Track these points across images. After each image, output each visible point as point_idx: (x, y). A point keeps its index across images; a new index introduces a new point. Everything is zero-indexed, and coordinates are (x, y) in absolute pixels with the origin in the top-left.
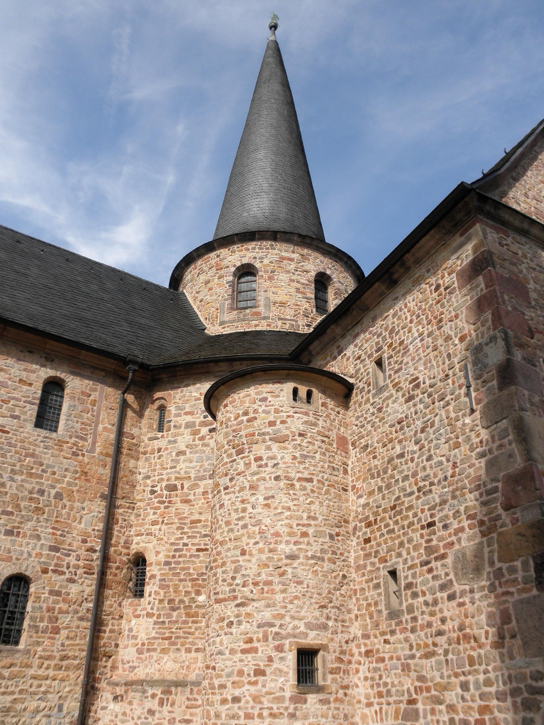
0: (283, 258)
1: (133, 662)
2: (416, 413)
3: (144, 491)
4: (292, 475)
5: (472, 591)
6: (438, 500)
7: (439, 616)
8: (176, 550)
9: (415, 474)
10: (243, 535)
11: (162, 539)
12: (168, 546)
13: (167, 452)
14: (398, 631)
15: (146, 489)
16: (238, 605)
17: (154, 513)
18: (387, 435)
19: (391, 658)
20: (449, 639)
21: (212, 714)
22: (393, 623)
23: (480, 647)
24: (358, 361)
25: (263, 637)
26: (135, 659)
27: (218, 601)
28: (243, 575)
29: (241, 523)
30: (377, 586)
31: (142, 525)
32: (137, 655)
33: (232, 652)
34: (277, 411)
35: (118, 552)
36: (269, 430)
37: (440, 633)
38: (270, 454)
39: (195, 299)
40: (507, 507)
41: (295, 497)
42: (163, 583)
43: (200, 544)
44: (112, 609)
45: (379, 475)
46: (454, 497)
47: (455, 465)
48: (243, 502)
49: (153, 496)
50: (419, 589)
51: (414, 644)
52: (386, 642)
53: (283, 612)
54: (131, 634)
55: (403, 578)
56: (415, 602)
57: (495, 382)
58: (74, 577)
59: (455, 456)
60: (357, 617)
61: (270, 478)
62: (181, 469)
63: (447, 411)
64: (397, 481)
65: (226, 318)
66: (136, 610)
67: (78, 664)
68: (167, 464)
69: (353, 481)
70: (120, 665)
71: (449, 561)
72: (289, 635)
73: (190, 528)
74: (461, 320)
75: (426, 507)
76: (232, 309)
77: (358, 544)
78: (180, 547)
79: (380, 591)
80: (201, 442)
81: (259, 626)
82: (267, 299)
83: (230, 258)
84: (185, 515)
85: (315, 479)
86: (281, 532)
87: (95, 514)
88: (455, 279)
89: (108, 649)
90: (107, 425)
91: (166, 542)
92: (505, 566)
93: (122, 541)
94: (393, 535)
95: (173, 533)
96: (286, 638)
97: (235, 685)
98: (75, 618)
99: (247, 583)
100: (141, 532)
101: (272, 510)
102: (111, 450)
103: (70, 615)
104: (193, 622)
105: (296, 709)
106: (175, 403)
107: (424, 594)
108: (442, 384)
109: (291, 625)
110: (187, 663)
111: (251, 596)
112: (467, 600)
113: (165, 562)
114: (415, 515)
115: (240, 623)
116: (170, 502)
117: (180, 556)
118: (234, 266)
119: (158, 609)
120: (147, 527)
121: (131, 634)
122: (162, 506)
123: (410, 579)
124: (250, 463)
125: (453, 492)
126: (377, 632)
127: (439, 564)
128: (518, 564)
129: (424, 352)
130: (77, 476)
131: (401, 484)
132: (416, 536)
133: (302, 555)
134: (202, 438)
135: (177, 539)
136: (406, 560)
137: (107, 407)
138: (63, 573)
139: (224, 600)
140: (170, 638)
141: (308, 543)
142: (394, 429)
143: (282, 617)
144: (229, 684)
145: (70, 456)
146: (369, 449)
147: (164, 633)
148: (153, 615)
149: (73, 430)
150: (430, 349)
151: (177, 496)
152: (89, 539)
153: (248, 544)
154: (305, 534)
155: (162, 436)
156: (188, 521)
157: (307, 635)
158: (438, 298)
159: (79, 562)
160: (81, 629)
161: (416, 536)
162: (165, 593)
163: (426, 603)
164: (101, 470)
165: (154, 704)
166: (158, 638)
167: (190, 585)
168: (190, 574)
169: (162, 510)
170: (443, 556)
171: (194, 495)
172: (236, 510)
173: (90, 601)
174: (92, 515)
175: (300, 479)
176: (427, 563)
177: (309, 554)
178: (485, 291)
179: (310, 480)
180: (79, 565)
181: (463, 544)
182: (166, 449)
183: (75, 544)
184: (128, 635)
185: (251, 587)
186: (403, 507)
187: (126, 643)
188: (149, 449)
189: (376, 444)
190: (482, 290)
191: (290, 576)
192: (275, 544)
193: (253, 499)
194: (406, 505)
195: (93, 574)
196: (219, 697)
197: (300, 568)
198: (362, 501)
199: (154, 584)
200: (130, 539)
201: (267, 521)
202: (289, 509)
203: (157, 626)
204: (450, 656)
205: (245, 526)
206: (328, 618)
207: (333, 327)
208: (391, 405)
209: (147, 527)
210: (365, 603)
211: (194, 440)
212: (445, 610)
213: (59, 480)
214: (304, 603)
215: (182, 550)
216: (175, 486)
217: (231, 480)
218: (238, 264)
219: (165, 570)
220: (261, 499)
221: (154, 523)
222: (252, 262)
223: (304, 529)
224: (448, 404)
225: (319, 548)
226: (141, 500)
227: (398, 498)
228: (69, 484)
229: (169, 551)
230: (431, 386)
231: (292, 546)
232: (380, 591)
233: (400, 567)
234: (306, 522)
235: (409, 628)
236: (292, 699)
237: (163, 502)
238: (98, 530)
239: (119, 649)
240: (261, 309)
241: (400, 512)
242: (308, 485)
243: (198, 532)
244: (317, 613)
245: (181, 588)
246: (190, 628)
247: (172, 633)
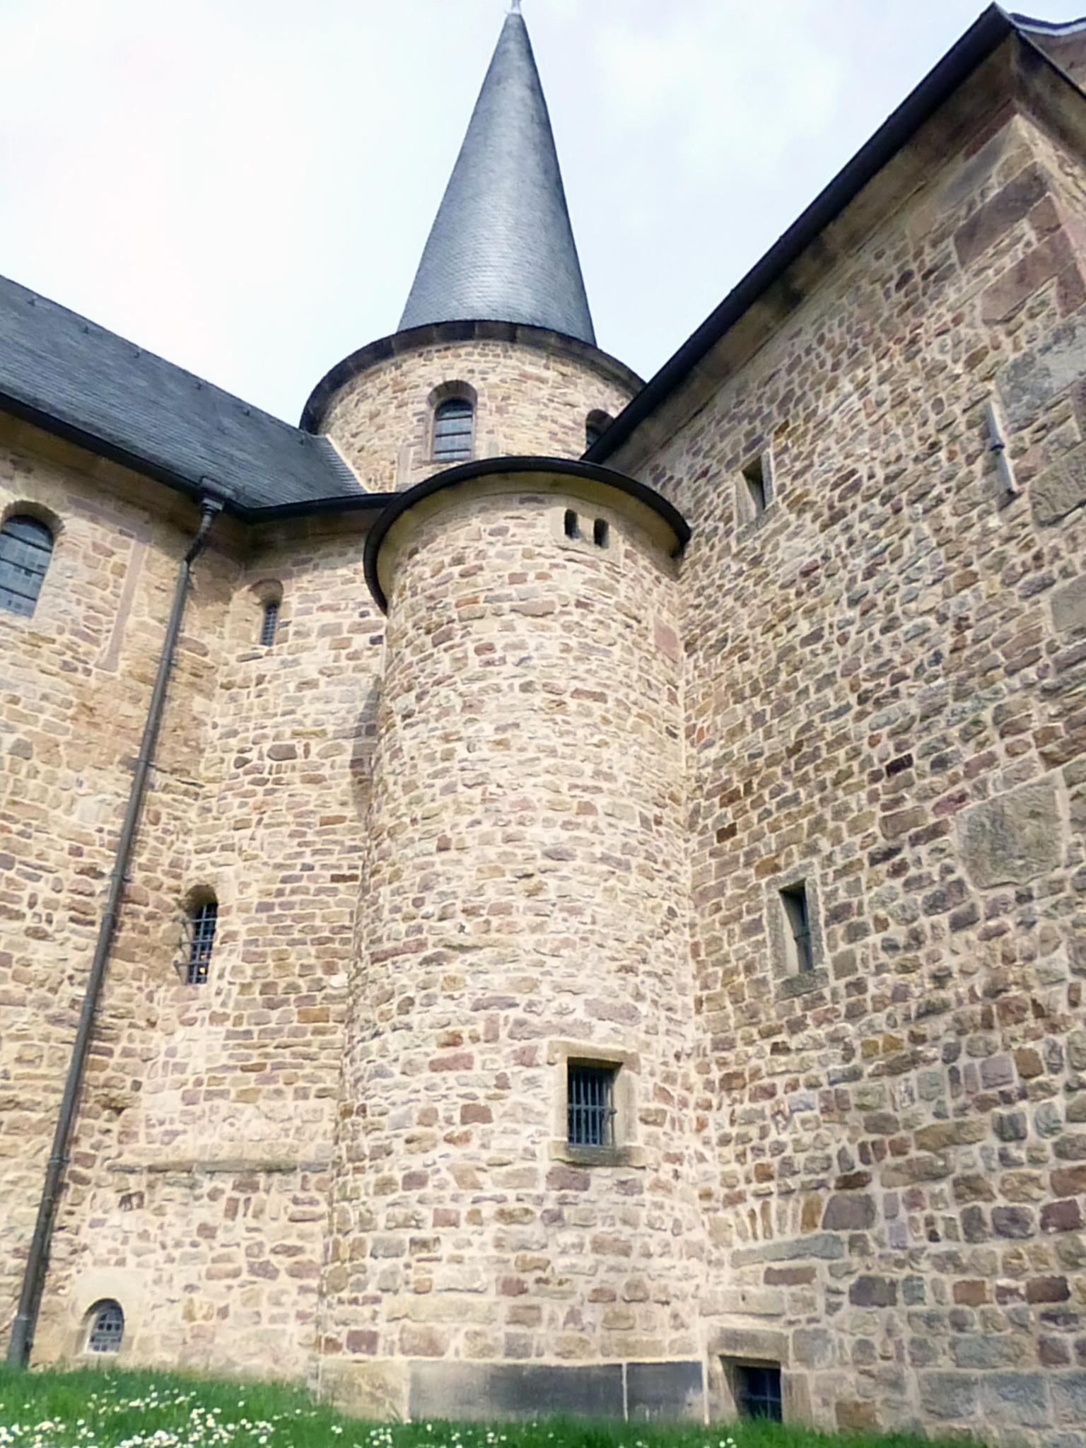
0: (525, 377)
1: (172, 1121)
2: (851, 542)
3: (222, 761)
4: (561, 683)
5: (1024, 898)
6: (915, 710)
7: (926, 969)
8: (284, 881)
10: (445, 807)
11: (255, 857)
12: (268, 871)
13: (276, 683)
14: (809, 1021)
15: (226, 756)
16: (427, 961)
17: (243, 805)
18: (774, 605)
19: (793, 1086)
20: (957, 1020)
21: (354, 1217)
22: (798, 1002)
23: (1054, 1028)
24: (703, 481)
25: (486, 1032)
26: (176, 1116)
27: (376, 959)
28: (441, 894)
29: (439, 783)
30: (755, 927)
31: (213, 830)
32: (181, 1107)
33: (410, 1068)
34: (528, 555)
35: (156, 884)
37: (931, 1010)
38: (511, 638)
39: (349, 446)
41: (567, 727)
42: (253, 949)
43: (339, 867)
44: (132, 1005)
45: (755, 690)
47: (961, 625)
48: (446, 738)
49: (241, 770)
50: (867, 918)
51: (857, 1044)
52: (776, 1049)
53: (534, 973)
54: (172, 1061)
55: (821, 899)
56: (858, 949)
58: (44, 925)
59: (962, 605)
60: (699, 1002)
61: (511, 686)
62: (305, 716)
66: (187, 1009)
67: (41, 1121)
68: (276, 705)
69: (688, 719)
70: (142, 1130)
71: (953, 840)
72: (550, 1028)
73: (318, 833)
74: (971, 325)
75: (885, 731)
77: (702, 845)
78: (296, 872)
79: (760, 937)
80: (352, 663)
81: (476, 1009)
83: (422, 371)
84: (311, 807)
85: (611, 696)
86: (534, 799)
87: (108, 797)
88: (952, 248)
89: (114, 1093)
90: (146, 619)
91: (265, 864)
93: (165, 860)
94: (794, 809)
95: (282, 843)
96: (538, 1034)
97: (414, 1146)
98: (41, 1019)
99: (450, 910)
100: (211, 844)
101: (513, 752)
102: (152, 671)
103: (29, 1010)
104: (316, 1032)
105: (562, 1202)
106: (299, 589)
107: (882, 924)
108: (920, 467)
109: (554, 1005)
110: (297, 1122)
111: (459, 939)
112: (1009, 921)
113: (260, 904)
114: (856, 753)
115: (430, 1001)
116: (277, 782)
117: (293, 892)
119: (237, 1006)
120: (223, 833)
121: (172, 1061)
122: (260, 790)
123: (842, 897)
124: (466, 657)
125: (960, 682)
126: (754, 1031)
127: (923, 850)
129: (868, 415)
130: (71, 712)
131: (813, 697)
133: (580, 852)
134: (353, 657)
135: (290, 857)
136: (829, 858)
137: (148, 584)
138: (19, 916)
139: (396, 952)
140: (259, 1068)
141: (595, 829)
142: (792, 591)
143: (533, 986)
144: (399, 1145)
145: (55, 669)
146: (729, 645)
147: (248, 1058)
148: (225, 1017)
149: (69, 618)
150: (887, 405)
151: (293, 768)
152: (86, 849)
153: (454, 826)
154: (587, 809)
155: (269, 654)
156: (315, 819)
157: (590, 1029)
158: (905, 301)
159: (60, 896)
160: (53, 1043)
162: (256, 969)
163: (890, 947)
164: (127, 709)
165: (210, 1213)
166: (235, 1068)
167: (313, 952)
168: (314, 930)
169: (260, 797)
170: (936, 831)
171: (332, 767)
172: (431, 758)
173: (80, 984)
174: (100, 797)
175: (577, 693)
176: (889, 853)
177: (598, 851)
178: (1035, 245)
179: (601, 698)
180: (57, 902)
181: (992, 794)
182: (276, 677)
183: (53, 855)
184: (166, 1064)
185: (461, 918)
186: (822, 744)
187: (159, 1080)
188: (238, 678)
189: (746, 632)
190: (1028, 244)
191: (552, 896)
192: (522, 824)
193: (469, 731)
194: (829, 737)
195: (92, 923)
196: (371, 1177)
197: (575, 879)
198: (713, 753)
199: (231, 952)
200: (185, 858)
201: (502, 776)
202: (552, 752)
203: (231, 1042)
204: (963, 1061)
205: (449, 789)
206: (639, 996)
207: (646, 424)
208: (783, 544)
209: (223, 833)
210: (720, 971)
211: (336, 659)
212: (945, 953)
213: (26, 716)
214: (585, 957)
215: (298, 879)
216: (291, 749)
217: (419, 698)
218: (439, 381)
219: (259, 920)
220: (488, 730)
222: (466, 378)
223: (587, 797)
224: (940, 500)
225: (618, 840)
226: (212, 780)
227: (809, 726)
228: (49, 727)
229: (270, 881)
230: (889, 479)
231: (557, 831)
232: (760, 937)
234: (591, 783)
235: (843, 1010)
236: (551, 1176)
237: (264, 782)
238: (110, 833)
239: (141, 1094)
241: (815, 754)
242: (596, 707)
243: (335, 842)
244: (614, 982)
245: (292, 960)
246: (308, 1044)
247: (267, 1055)
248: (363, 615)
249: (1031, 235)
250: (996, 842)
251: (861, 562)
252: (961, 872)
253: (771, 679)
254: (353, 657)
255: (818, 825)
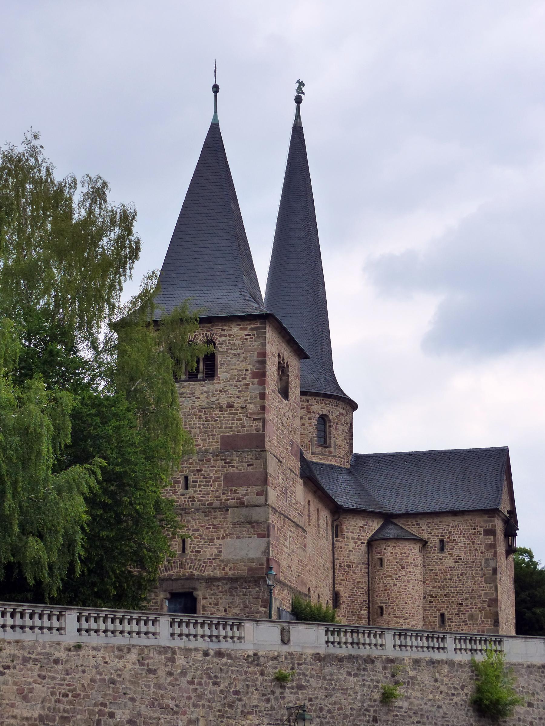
0: (340, 413)
5: (474, 624)
8: (353, 592)
9: (456, 587)
17: (343, 576)
27: (394, 617)
29: (405, 593)
30: (436, 617)
36: (413, 562)
40: (488, 606)
45: (439, 582)
46: (471, 598)
47: (473, 590)
48: (405, 586)
50: (454, 621)
57: (491, 572)
63: (472, 573)
64: (448, 587)
65: (316, 451)
71: (467, 615)
76: (319, 445)
82: (335, 443)
92: (485, 620)
107: (456, 622)
115: (405, 625)
118: (318, 413)
128: (489, 620)
132: (454, 606)
134: (358, 546)
148: (345, 616)
161: (454, 606)
163: (456, 625)
170: (465, 614)
172: (403, 588)
198: (429, 588)
205: (406, 594)
217: (399, 577)
218: (321, 413)
221: (343, 580)
227: (448, 593)
233: (446, 613)
237: (346, 572)
240: (332, 449)
248: (359, 536)
249: (492, 540)
250: (471, 617)
251: (460, 572)
252: (467, 619)
253: (442, 582)
254: (358, 546)
255: (448, 607)
